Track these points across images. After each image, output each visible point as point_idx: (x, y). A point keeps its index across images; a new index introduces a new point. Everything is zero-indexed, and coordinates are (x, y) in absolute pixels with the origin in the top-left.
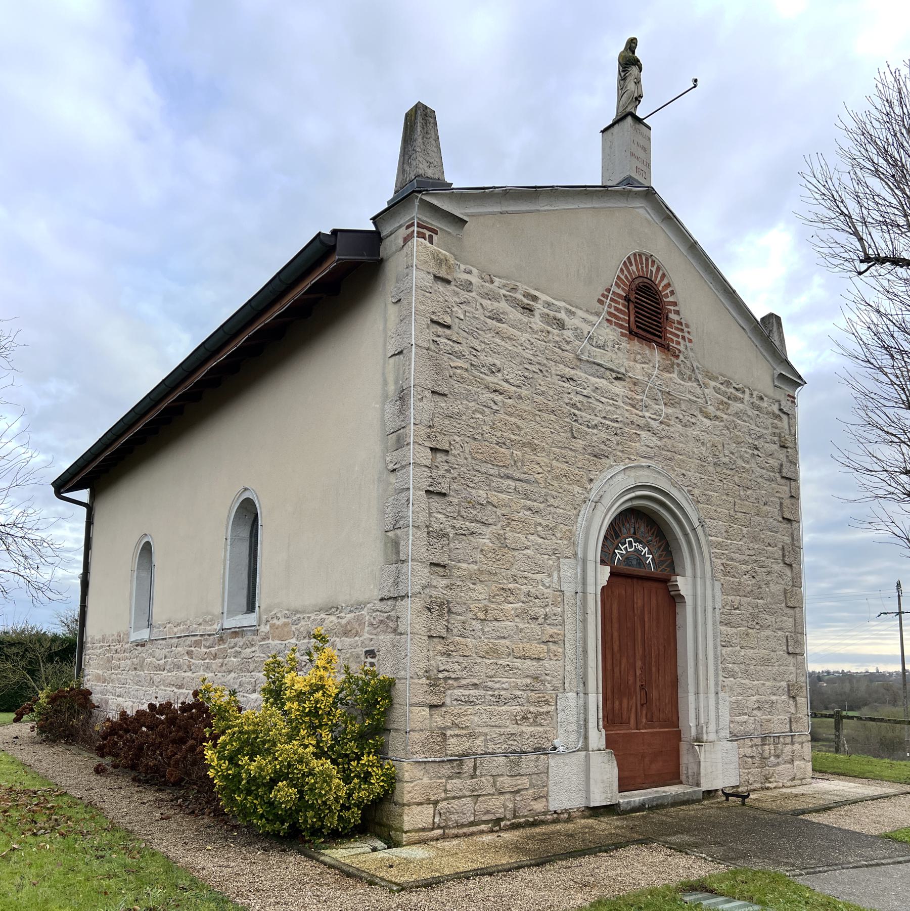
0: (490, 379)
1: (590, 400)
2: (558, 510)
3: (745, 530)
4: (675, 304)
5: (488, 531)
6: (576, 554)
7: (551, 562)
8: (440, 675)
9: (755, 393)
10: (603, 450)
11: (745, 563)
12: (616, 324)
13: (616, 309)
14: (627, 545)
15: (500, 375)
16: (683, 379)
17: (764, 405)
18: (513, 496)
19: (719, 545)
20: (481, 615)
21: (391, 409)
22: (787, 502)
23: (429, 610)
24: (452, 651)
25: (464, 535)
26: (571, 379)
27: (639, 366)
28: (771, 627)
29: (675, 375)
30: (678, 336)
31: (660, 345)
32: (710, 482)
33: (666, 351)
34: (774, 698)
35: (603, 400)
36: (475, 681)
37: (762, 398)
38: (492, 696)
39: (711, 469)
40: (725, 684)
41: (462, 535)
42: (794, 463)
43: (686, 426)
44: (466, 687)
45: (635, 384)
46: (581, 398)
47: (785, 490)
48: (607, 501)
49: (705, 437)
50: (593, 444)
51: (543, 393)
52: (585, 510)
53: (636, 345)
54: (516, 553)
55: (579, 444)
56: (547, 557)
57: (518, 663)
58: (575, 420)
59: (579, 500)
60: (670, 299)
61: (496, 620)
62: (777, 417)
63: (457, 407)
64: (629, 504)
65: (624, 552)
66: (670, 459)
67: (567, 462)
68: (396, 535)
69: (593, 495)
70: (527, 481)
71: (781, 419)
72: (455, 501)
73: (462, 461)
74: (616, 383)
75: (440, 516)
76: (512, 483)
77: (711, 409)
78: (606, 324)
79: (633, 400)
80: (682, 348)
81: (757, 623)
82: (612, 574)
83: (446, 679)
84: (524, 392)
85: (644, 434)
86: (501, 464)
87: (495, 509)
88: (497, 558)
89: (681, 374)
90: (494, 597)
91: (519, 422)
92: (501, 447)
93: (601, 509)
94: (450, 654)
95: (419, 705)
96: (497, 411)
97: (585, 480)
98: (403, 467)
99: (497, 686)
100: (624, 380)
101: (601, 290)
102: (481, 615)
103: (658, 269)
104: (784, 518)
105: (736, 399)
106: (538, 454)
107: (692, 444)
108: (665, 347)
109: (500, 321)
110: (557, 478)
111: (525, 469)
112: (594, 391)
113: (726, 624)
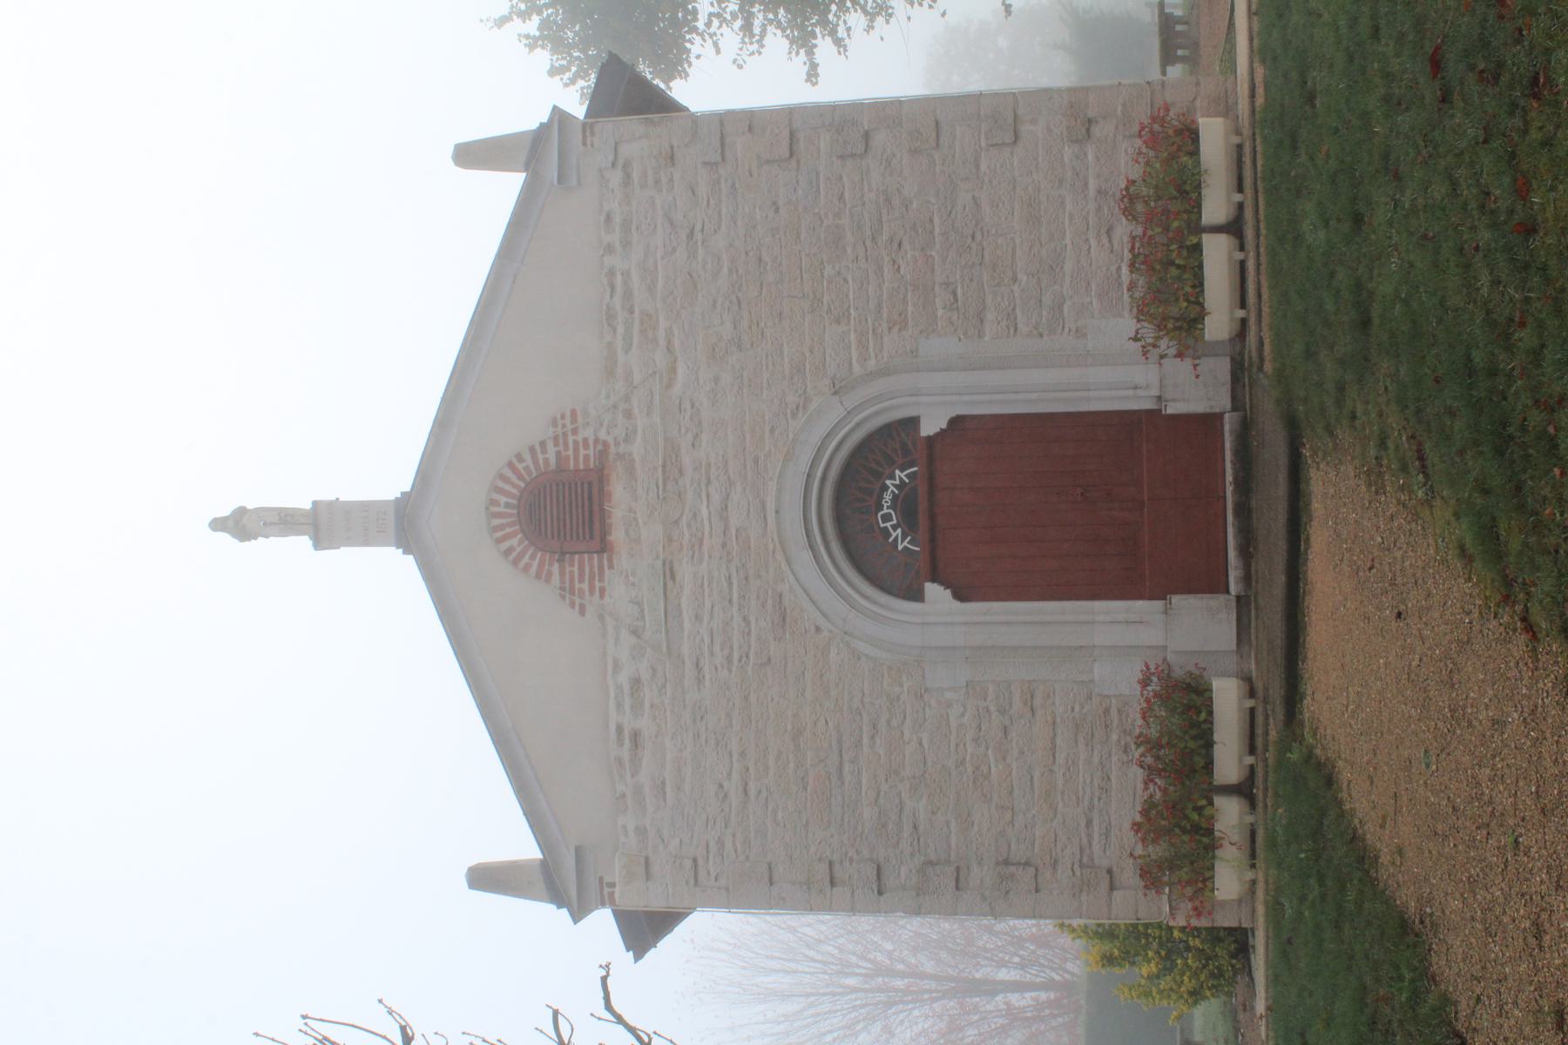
3: (828, 271)
7: (933, 702)
8: (1078, 873)
10: (774, 606)
12: (601, 579)
14: (888, 525)
15: (726, 784)
16: (635, 431)
23: (1007, 892)
24: (1051, 858)
25: (918, 840)
26: (697, 665)
30: (576, 442)
32: (771, 367)
33: (605, 472)
34: (1093, 185)
36: (1083, 824)
37: (608, 219)
41: (918, 840)
44: (1090, 836)
54: (930, 763)
56: (927, 710)
57: (1061, 758)
58: (747, 657)
61: (1011, 793)
65: (899, 531)
66: (756, 461)
67: (803, 673)
70: (840, 741)
74: (678, 577)
75: (902, 874)
76: (847, 767)
79: (693, 546)
81: (973, 237)
82: (934, 579)
83: (1081, 866)
86: (827, 782)
87: (882, 794)
88: (938, 790)
90: (986, 797)
92: (807, 783)
94: (1055, 861)
95: (1109, 906)
96: (768, 790)
100: (671, 562)
102: (1008, 815)
104: (791, 155)
106: (804, 724)
113: (982, 322)
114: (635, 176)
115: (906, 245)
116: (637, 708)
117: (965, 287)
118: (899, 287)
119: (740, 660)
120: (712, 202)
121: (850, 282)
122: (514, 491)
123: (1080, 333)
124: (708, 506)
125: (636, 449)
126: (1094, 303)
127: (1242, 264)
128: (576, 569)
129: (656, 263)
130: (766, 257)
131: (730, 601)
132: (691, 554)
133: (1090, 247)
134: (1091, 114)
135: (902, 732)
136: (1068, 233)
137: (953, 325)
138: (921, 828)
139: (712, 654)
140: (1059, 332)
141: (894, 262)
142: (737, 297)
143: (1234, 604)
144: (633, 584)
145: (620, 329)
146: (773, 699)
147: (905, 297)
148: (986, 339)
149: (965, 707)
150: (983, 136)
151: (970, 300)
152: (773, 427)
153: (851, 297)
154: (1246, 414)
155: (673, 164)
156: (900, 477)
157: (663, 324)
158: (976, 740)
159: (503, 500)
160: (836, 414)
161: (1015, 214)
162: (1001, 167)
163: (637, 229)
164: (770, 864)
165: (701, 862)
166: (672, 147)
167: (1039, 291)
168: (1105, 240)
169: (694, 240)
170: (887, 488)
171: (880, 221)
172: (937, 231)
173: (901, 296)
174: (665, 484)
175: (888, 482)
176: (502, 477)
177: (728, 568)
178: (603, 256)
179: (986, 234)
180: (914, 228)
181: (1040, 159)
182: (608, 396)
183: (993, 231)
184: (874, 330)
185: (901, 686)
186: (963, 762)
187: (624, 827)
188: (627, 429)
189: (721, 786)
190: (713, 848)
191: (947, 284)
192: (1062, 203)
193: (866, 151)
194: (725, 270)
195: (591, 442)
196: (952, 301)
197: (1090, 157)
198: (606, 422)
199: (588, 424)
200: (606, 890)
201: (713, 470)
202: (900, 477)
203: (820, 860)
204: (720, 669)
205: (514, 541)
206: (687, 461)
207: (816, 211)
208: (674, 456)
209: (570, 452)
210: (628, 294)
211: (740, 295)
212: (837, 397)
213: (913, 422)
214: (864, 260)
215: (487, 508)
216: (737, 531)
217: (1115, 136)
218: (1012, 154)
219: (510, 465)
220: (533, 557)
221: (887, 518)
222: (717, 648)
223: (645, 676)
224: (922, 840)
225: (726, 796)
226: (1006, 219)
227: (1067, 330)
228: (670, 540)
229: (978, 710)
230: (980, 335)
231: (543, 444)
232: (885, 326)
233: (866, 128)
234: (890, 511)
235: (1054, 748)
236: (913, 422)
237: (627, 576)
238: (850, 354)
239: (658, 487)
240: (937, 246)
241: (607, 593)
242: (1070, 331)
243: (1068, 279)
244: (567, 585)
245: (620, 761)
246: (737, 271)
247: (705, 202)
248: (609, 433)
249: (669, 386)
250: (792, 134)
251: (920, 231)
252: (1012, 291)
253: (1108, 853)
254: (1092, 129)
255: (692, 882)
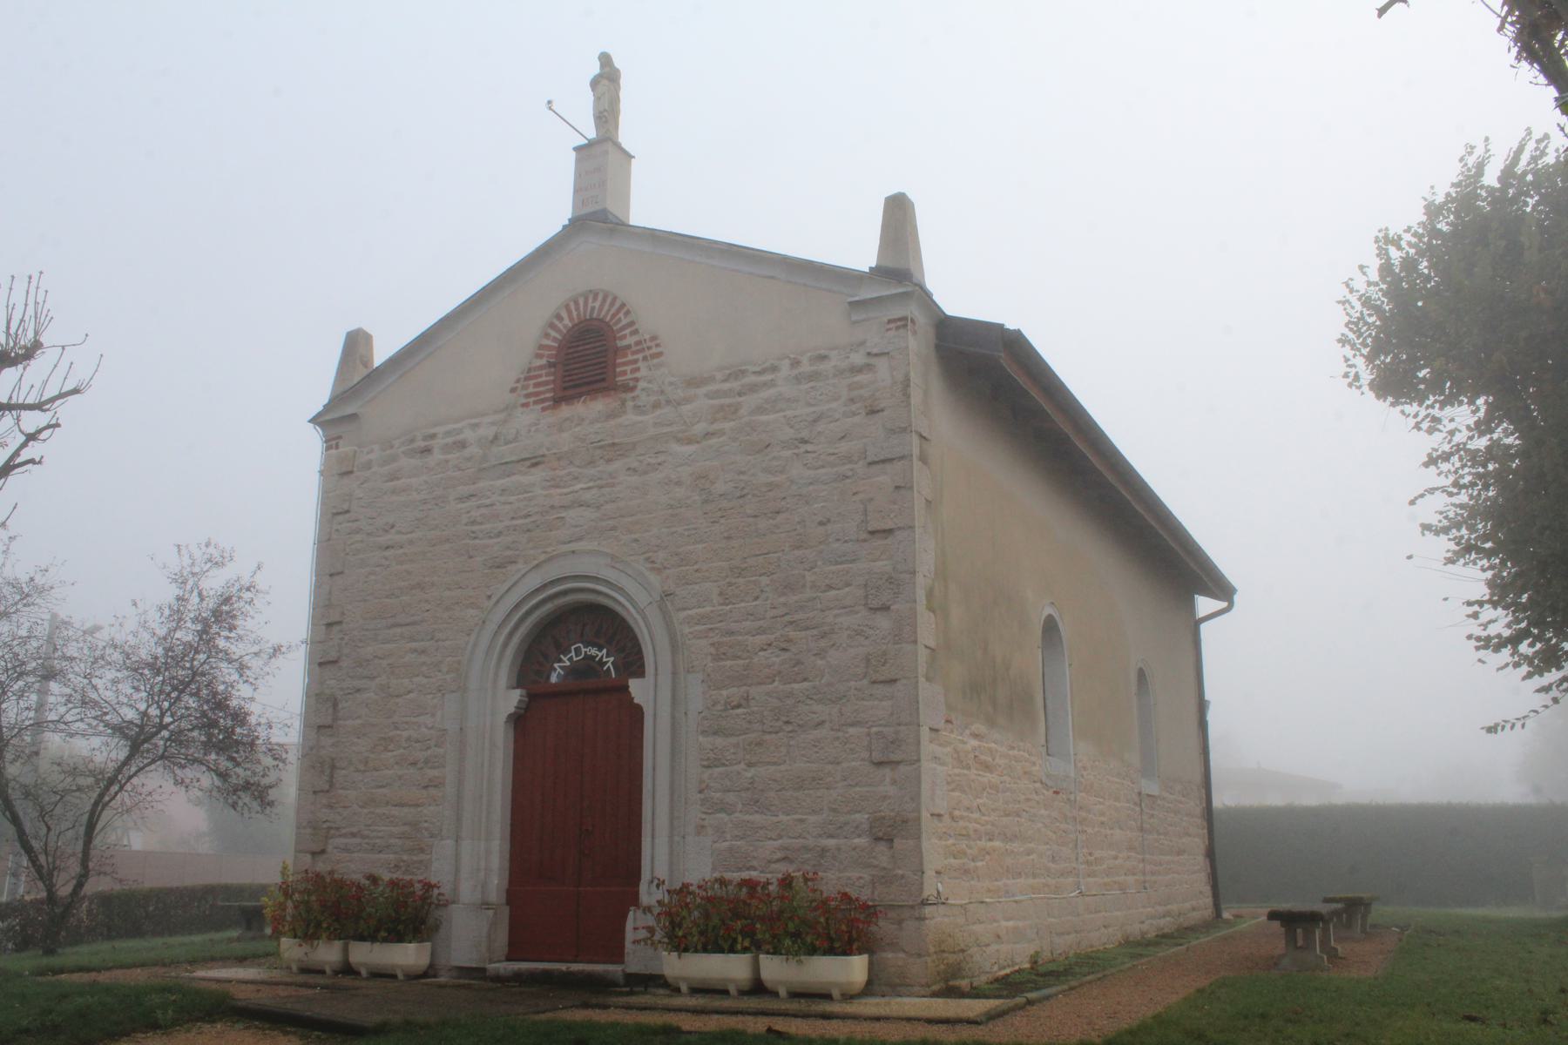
1: (495, 507)
2: (448, 643)
3: (765, 580)
7: (435, 701)
11: (761, 631)
12: (535, 403)
14: (573, 654)
15: (393, 531)
20: (362, 767)
28: (827, 725)
30: (636, 361)
32: (686, 533)
33: (612, 392)
35: (512, 499)
36: (355, 830)
37: (823, 358)
38: (367, 844)
40: (706, 823)
41: (349, 693)
43: (646, 473)
44: (344, 836)
45: (559, 459)
50: (495, 555)
56: (432, 696)
57: (395, 811)
58: (475, 538)
65: (568, 663)
66: (614, 528)
74: (533, 470)
76: (399, 630)
81: (787, 722)
83: (330, 828)
99: (375, 834)
100: (543, 463)
102: (362, 767)
104: (872, 533)
112: (501, 495)
114: (859, 378)
115: (786, 655)
116: (446, 449)
117: (744, 716)
118: (748, 651)
119: (473, 532)
120: (832, 458)
121: (755, 603)
122: (603, 313)
123: (701, 829)
124: (582, 489)
125: (630, 417)
126: (724, 844)
127: (725, 992)
128: (544, 379)
129: (782, 410)
130: (780, 518)
131: (513, 518)
132: (548, 478)
133: (774, 840)
134: (897, 841)
135: (418, 676)
136: (789, 817)
137: (713, 705)
138: (358, 695)
139: (478, 507)
140: (703, 810)
141: (770, 645)
142: (748, 494)
143: (481, 965)
144: (530, 431)
145: (727, 386)
146: (445, 563)
147: (739, 657)
148: (701, 738)
149: (432, 728)
150: (880, 729)
151: (732, 722)
152: (638, 541)
153: (743, 604)
154: (621, 987)
155: (867, 414)
156: (607, 662)
157: (727, 425)
158: (409, 739)
159: (597, 305)
160: (642, 598)
161: (808, 764)
162: (851, 750)
163: (812, 388)
164: (342, 573)
165: (347, 515)
166: (882, 410)
167: (738, 789)
168: (779, 855)
169: (801, 445)
170: (600, 650)
171: (807, 628)
172: (796, 686)
173: (739, 654)
174: (601, 447)
175: (605, 651)
176: (615, 299)
177: (537, 513)
178: (790, 359)
179: (791, 735)
180: (798, 663)
181: (858, 789)
182: (671, 384)
183: (791, 743)
184: (711, 629)
185: (448, 672)
186: (397, 728)
187: (372, 451)
188: (644, 406)
189: (393, 527)
191: (747, 699)
192: (814, 812)
193: (871, 609)
194: (772, 479)
195: (637, 375)
196: (732, 704)
197: (856, 841)
198: (650, 386)
199: (650, 369)
200: (334, 442)
201: (608, 489)
202: (607, 662)
203: (343, 614)
204: (469, 515)
205: (567, 321)
206: (616, 465)
207: (819, 563)
208: (621, 453)
209: (630, 357)
210: (753, 388)
211: (750, 496)
212: (659, 599)
213: (640, 672)
214: (772, 615)
215: (591, 291)
216: (563, 518)
217: (875, 867)
218: (863, 760)
219: (623, 305)
220: (555, 339)
221: (578, 651)
222: (483, 511)
223: (467, 452)
224: (350, 696)
225: (387, 531)
226: (803, 755)
227: (704, 816)
228: (559, 459)
229: (429, 740)
230: (703, 732)
231: (636, 332)
232: (715, 640)
233: (892, 607)
234: (583, 653)
235: (402, 805)
236: (640, 672)
237: (536, 424)
238: (694, 608)
239: (599, 441)
240: (781, 687)
241: (525, 409)
242: (704, 819)
243: (747, 817)
244: (532, 374)
245: (412, 441)
246: (770, 491)
247: (831, 451)
248: (643, 390)
249: (678, 440)
250: (890, 531)
251: (796, 669)
252: (740, 763)
253: (335, 850)
254: (883, 843)
255: (334, 511)
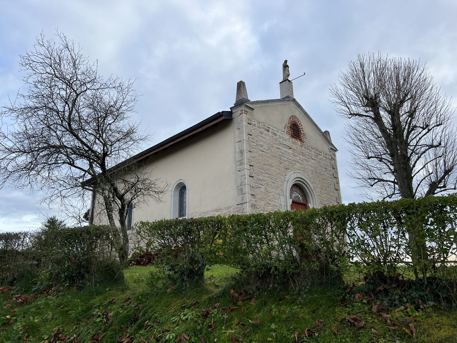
0: (261, 148)
3: (325, 192)
4: (302, 128)
5: (263, 187)
6: (284, 195)
9: (325, 153)
13: (288, 130)
16: (306, 149)
17: (327, 156)
18: (268, 178)
19: (319, 196)
20: (263, 209)
21: (237, 155)
22: (336, 184)
27: (295, 145)
29: (303, 148)
31: (299, 140)
39: (315, 174)
42: (337, 173)
46: (282, 153)
47: (335, 181)
48: (290, 181)
49: (312, 165)
51: (273, 152)
52: (285, 183)
53: (294, 140)
55: (282, 165)
59: (283, 180)
60: (301, 127)
62: (331, 160)
63: (254, 155)
64: (295, 183)
68: (242, 187)
69: (287, 179)
71: (332, 161)
72: (255, 179)
73: (256, 169)
74: (290, 150)
76: (268, 175)
77: (313, 157)
78: (286, 134)
80: (305, 140)
84: (269, 151)
85: (297, 163)
89: (305, 147)
91: (268, 159)
93: (289, 183)
97: (284, 175)
98: (243, 170)
101: (284, 125)
102: (263, 209)
103: (297, 119)
105: (320, 155)
107: (309, 167)
108: (301, 140)
109: (262, 134)
110: (278, 174)
111: (270, 171)
190: (253, 140)
